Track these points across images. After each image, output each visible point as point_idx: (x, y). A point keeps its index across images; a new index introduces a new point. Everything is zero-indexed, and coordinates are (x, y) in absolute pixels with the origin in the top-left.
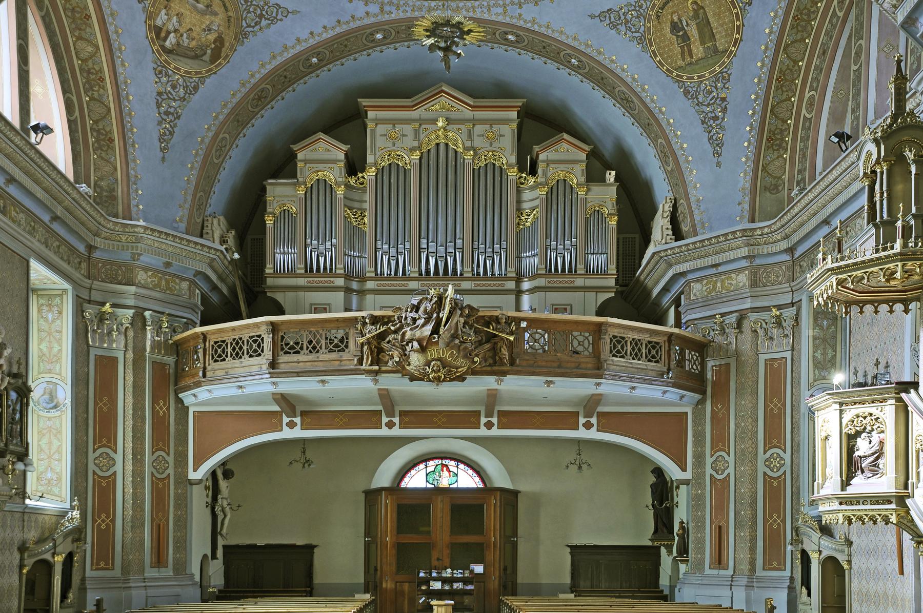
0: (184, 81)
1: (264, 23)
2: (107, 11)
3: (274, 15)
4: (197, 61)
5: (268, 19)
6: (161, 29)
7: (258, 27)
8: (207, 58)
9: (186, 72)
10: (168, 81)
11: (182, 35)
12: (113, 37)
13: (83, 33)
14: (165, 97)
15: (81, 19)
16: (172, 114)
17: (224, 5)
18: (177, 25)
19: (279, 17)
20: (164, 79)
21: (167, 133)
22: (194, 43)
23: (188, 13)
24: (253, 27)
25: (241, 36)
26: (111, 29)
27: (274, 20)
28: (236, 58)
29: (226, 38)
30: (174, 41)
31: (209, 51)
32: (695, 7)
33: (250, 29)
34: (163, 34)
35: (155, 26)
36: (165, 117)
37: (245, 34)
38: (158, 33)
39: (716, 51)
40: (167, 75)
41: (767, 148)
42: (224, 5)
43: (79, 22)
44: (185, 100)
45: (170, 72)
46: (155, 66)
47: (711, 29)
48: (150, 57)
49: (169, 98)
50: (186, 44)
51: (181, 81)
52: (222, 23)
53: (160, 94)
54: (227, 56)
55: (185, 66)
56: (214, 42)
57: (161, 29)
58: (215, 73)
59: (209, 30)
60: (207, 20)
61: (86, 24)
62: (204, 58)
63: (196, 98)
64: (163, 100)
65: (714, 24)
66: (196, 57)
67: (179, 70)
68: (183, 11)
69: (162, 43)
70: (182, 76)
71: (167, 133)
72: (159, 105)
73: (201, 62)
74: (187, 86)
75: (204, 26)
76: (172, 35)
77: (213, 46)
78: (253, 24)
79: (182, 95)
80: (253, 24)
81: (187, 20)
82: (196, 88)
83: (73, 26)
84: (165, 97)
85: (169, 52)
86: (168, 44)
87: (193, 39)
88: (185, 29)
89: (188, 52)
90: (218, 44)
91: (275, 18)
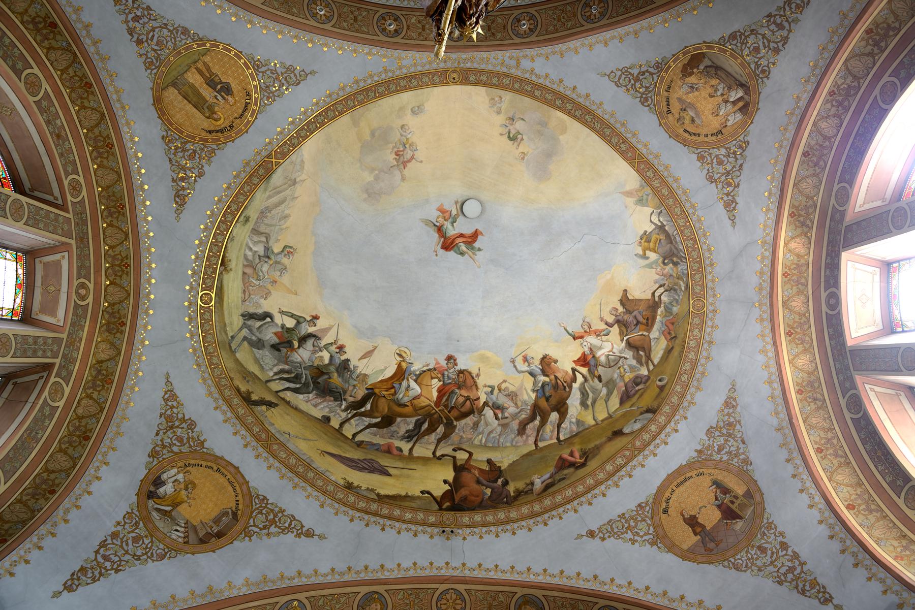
0: (742, 50)
1: (635, 72)
2: (784, 152)
3: (623, 76)
4: (719, 64)
5: (630, 73)
6: (740, 110)
7: (643, 69)
8: (706, 62)
9: (736, 58)
10: (760, 58)
11: (722, 95)
12: (792, 129)
13: (820, 142)
14: (772, 45)
15: (814, 154)
16: (774, 23)
17: (668, 104)
18: (723, 106)
19: (619, 73)
20: (763, 62)
21: (793, 6)
22: (714, 82)
23: (706, 112)
24: (647, 71)
25: (661, 66)
26: (790, 135)
27: (625, 71)
28: (676, 48)
29: (678, 71)
30: (733, 93)
31: (702, 67)
32: (215, 116)
33: (652, 70)
34: (741, 104)
35: (744, 114)
36: (786, 24)
37: (658, 67)
38: (746, 108)
39: (174, 84)
40: (758, 65)
41: (48, 16)
42: (668, 104)
43: (817, 153)
44: (752, 31)
45: (753, 66)
46: (765, 80)
47: (190, 102)
48: (765, 92)
49: (769, 41)
50: (722, 85)
51: (746, 52)
52: (677, 88)
53: (777, 51)
54: (684, 54)
55: (732, 66)
56: (691, 74)
57: (740, 110)
58: (704, 42)
59: (692, 87)
60: (691, 98)
61: (812, 148)
62: (710, 63)
63: (736, 27)
64: (776, 43)
65: (189, 107)
66: (717, 68)
67: (741, 64)
68: (711, 117)
69: (746, 97)
70: (742, 57)
71: (793, 6)
72: (785, 40)
73: (716, 61)
74: (742, 44)
75: (696, 93)
76: (732, 100)
77: (695, 70)
78: (647, 74)
79: (753, 37)
80: (647, 74)
81: (710, 106)
82: (733, 36)
83: (825, 152)
84: (772, 45)
85: (741, 85)
86: (740, 93)
87: (712, 86)
88: (716, 99)
89: (723, 76)
90: (689, 71)
91: (623, 73)
